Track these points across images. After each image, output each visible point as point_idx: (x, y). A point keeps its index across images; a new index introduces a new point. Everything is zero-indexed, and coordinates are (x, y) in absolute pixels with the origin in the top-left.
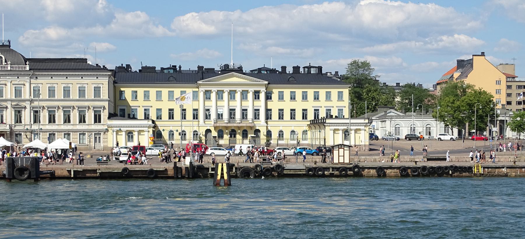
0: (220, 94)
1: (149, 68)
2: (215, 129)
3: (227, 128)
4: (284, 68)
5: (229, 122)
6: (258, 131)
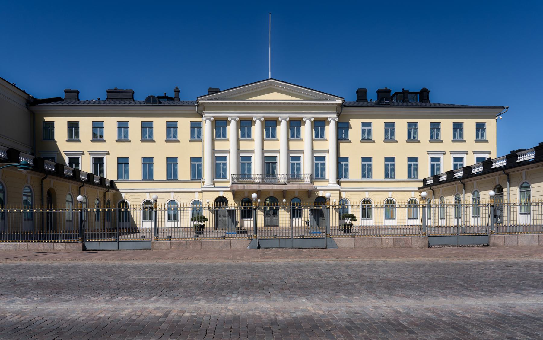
0: (245, 126)
2: (234, 197)
5: (264, 183)
6: (323, 200)
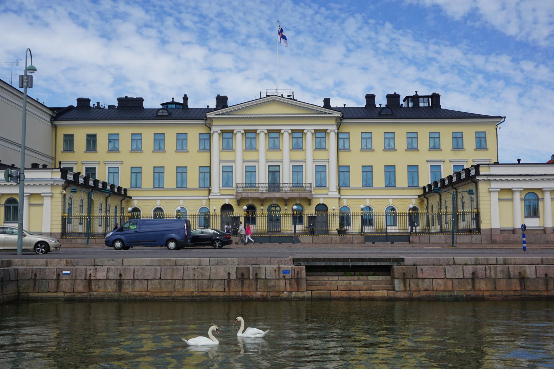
1: (132, 99)
3: (262, 201)
4: (370, 98)
